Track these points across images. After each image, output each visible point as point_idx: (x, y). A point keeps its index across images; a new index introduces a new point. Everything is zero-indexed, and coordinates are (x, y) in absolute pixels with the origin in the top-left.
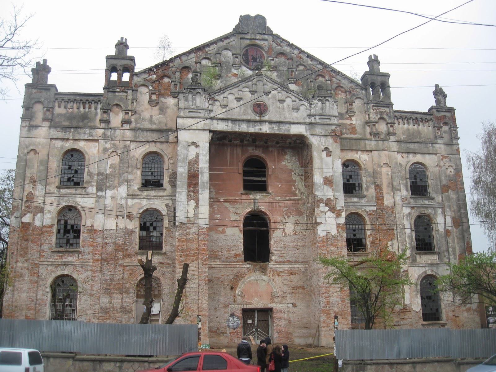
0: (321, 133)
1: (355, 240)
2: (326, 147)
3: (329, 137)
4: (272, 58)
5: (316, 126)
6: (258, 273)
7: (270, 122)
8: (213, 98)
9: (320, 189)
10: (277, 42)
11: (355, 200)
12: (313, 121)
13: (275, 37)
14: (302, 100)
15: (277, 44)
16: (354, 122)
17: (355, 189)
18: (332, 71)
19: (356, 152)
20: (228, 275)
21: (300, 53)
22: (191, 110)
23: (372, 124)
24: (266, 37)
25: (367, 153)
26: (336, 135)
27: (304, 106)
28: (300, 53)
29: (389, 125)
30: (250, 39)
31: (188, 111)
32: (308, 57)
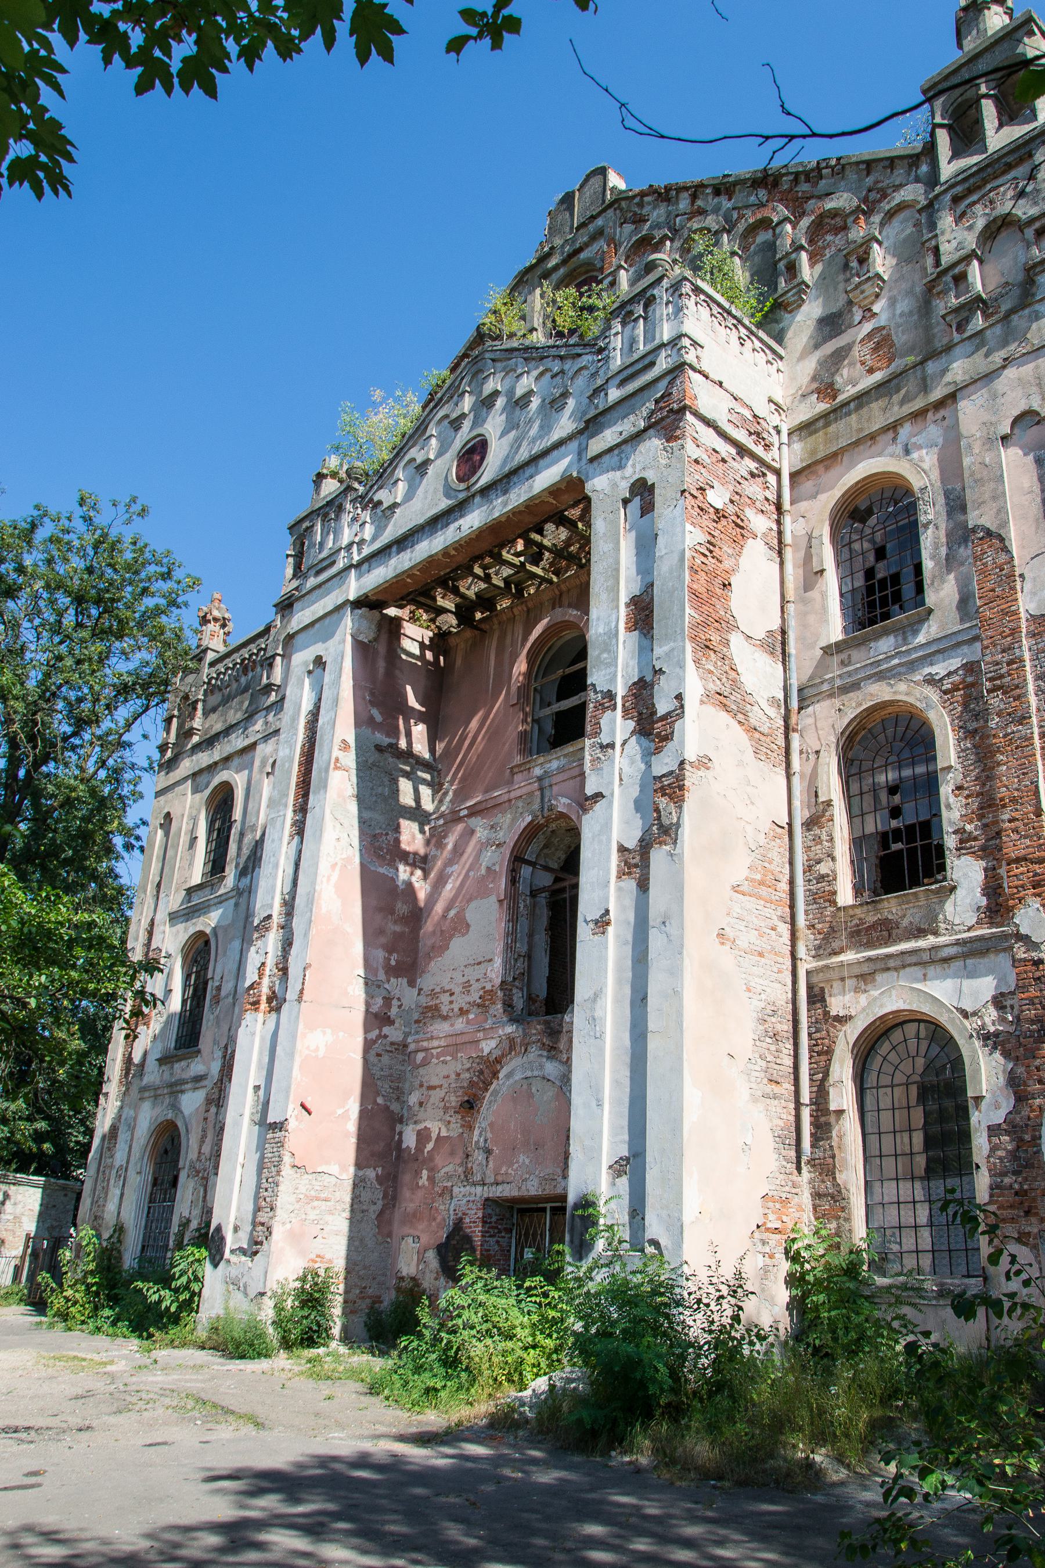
0: (621, 433)
1: (897, 834)
2: (637, 477)
3: (651, 431)
4: (610, 279)
5: (602, 419)
6: (534, 1051)
7: (485, 491)
8: (371, 500)
9: (605, 655)
10: (635, 214)
11: (885, 645)
12: (601, 408)
13: (623, 204)
14: (579, 355)
15: (634, 223)
16: (882, 320)
17: (897, 597)
18: (796, 181)
19: (891, 434)
20: (458, 1075)
21: (694, 197)
22: (320, 566)
23: (948, 278)
24: (599, 222)
25: (942, 413)
26: (671, 410)
27: (585, 372)
28: (694, 197)
29: (1030, 233)
30: (564, 262)
31: (313, 572)
32: (717, 192)
